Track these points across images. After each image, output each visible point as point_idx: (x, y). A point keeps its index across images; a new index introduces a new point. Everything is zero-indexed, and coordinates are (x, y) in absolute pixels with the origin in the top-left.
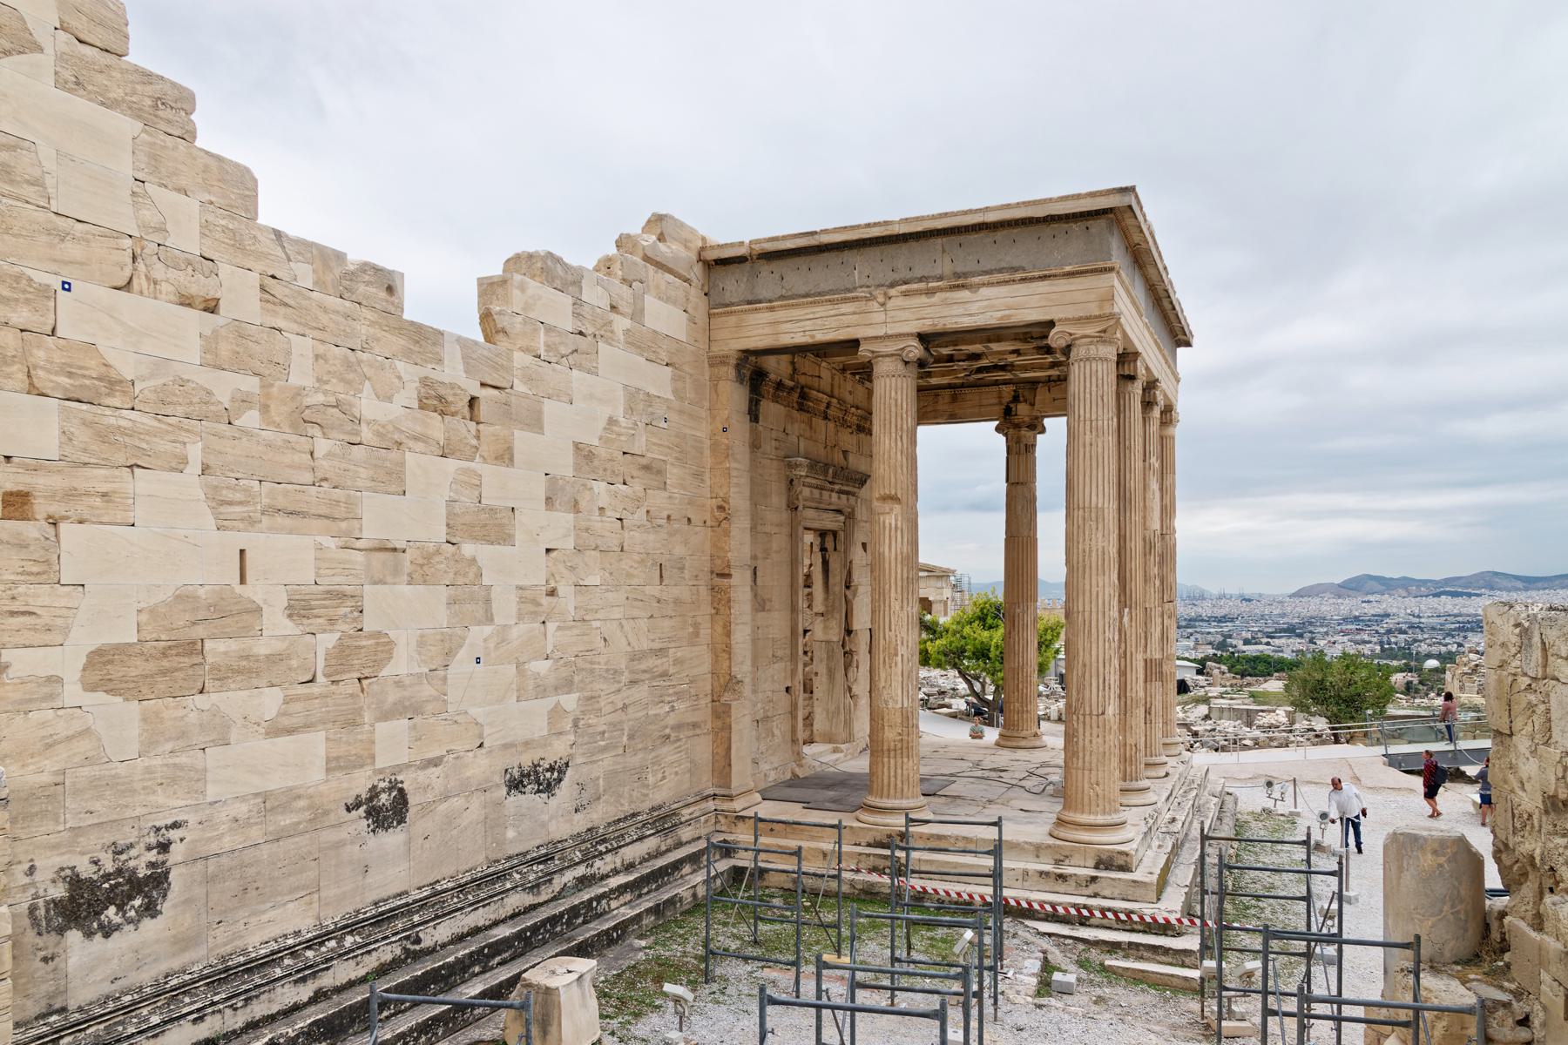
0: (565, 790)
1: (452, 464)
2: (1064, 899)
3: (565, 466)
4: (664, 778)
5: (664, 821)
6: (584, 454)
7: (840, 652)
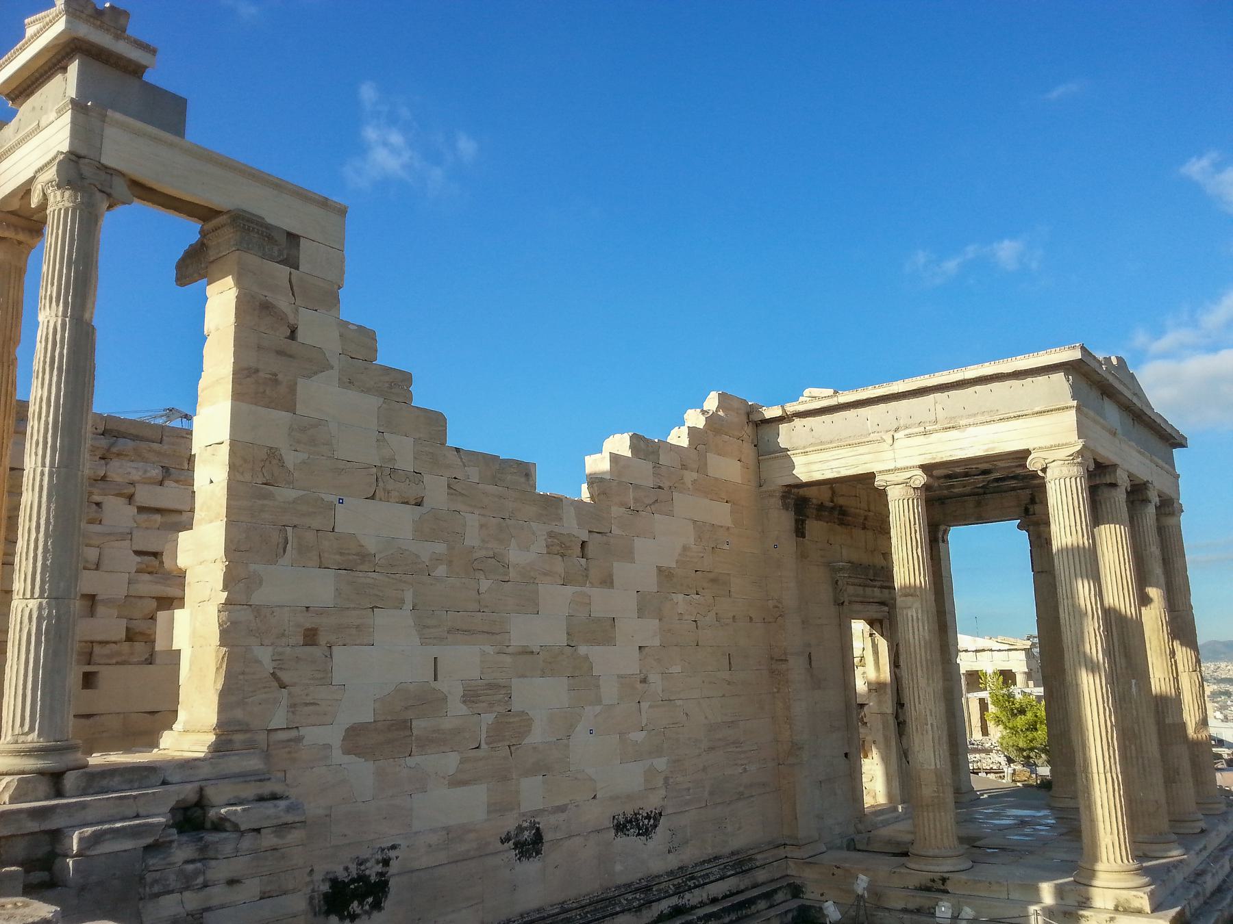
0: (660, 835)
1: (570, 590)
3: (650, 583)
4: (740, 828)
5: (741, 863)
6: (664, 574)
7: (891, 721)
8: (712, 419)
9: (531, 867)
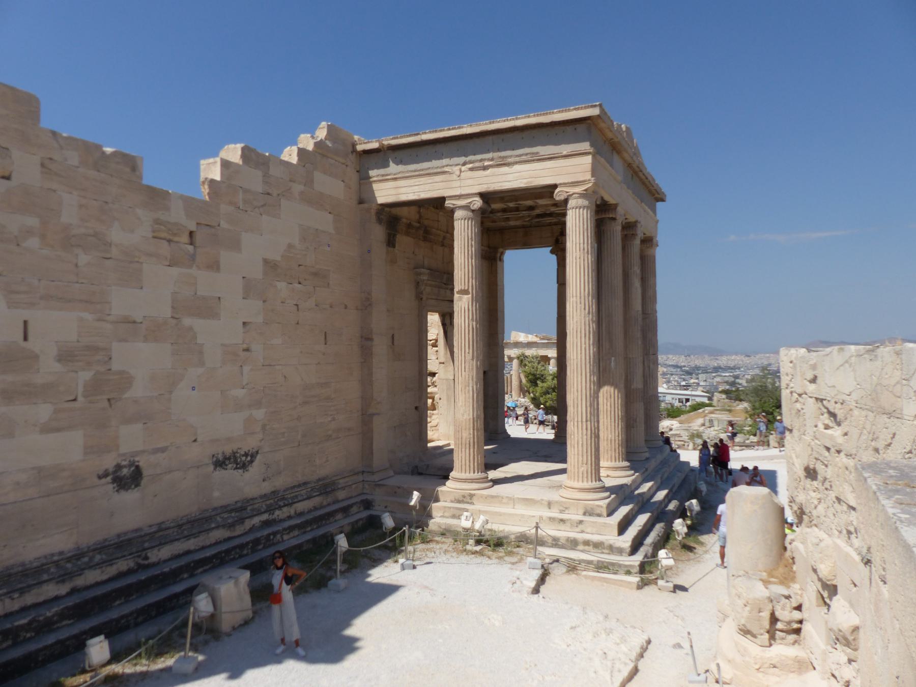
1: (175, 271)
2: (563, 533)
4: (327, 461)
5: (326, 487)
6: (270, 266)
8: (319, 145)
9: (130, 496)
